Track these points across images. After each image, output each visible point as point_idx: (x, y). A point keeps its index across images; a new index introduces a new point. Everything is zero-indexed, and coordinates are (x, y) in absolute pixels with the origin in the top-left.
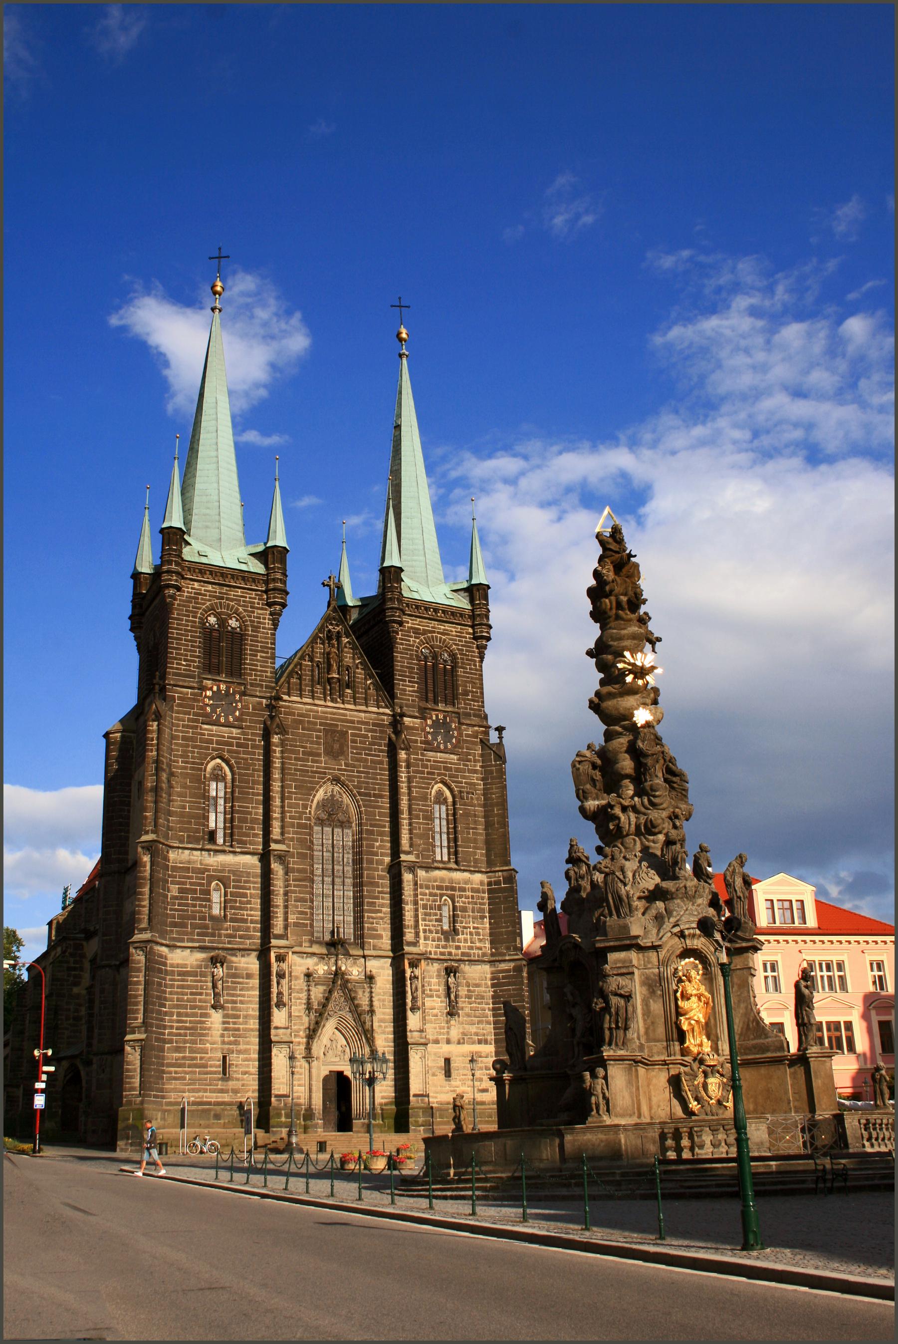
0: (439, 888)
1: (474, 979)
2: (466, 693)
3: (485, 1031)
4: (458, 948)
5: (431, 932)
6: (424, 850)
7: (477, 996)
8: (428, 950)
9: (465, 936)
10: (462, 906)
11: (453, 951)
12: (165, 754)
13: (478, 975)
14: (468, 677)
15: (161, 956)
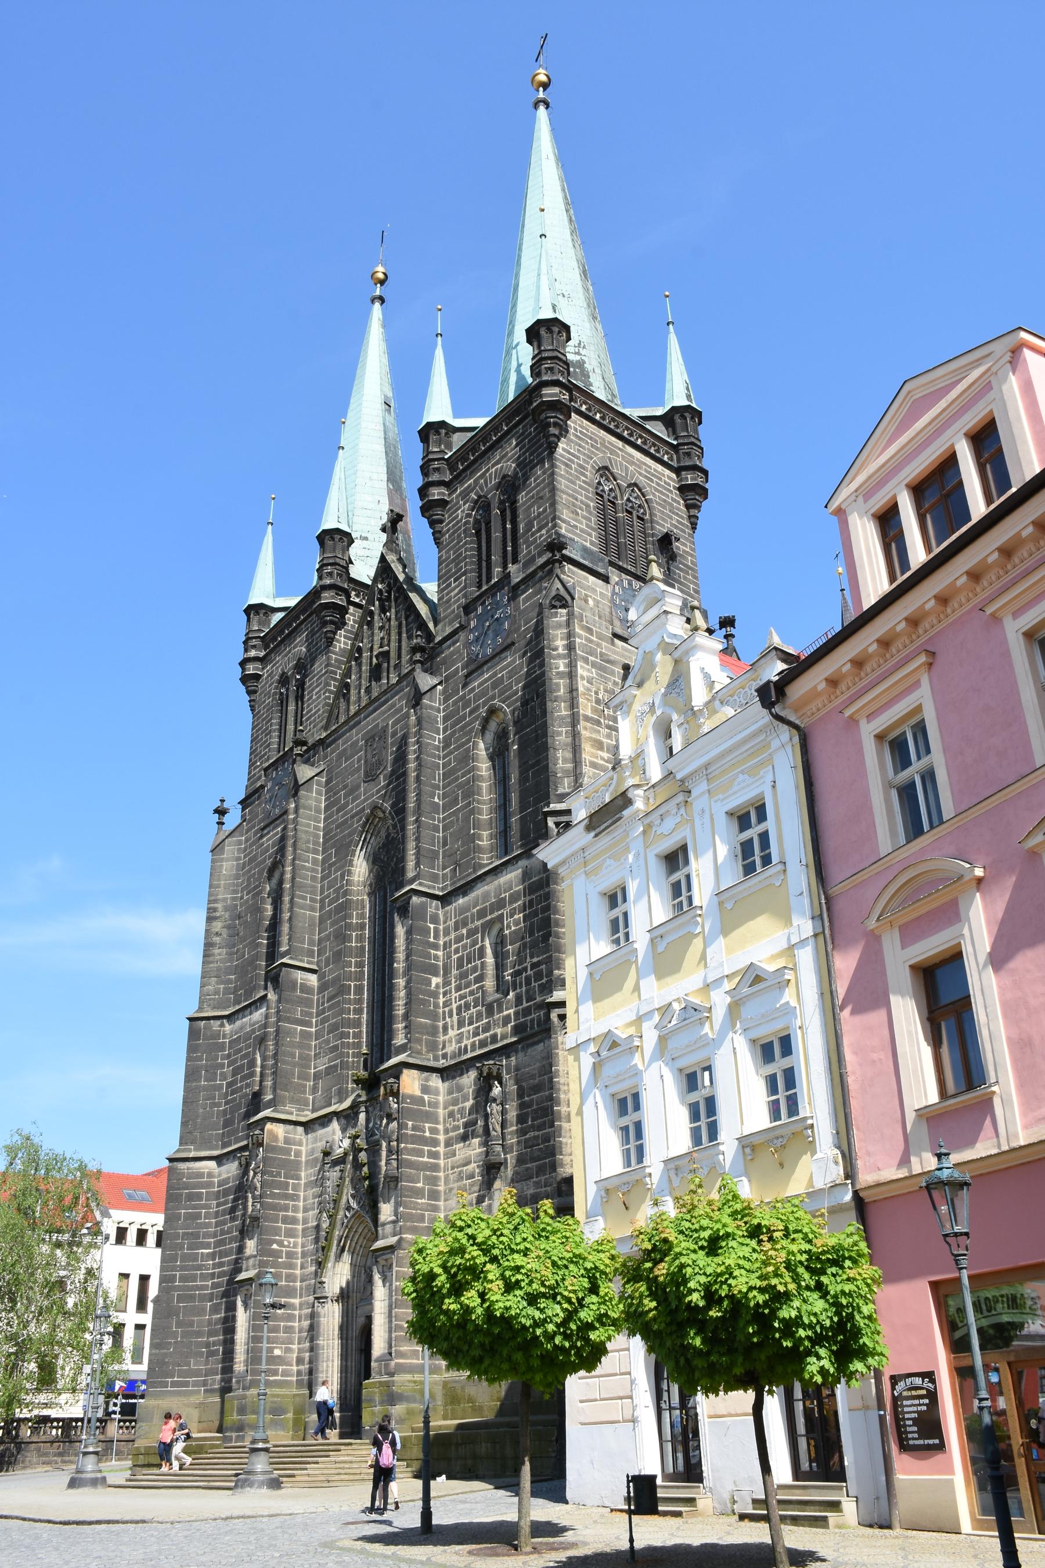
0: (482, 914)
1: (532, 1077)
2: (529, 525)
3: (549, 1189)
4: (506, 1020)
5: (467, 1006)
6: (463, 856)
7: (536, 1111)
8: (463, 1045)
9: (518, 990)
10: (514, 931)
11: (499, 1031)
12: (220, 897)
13: (538, 1065)
14: (533, 497)
15: (201, 1175)
